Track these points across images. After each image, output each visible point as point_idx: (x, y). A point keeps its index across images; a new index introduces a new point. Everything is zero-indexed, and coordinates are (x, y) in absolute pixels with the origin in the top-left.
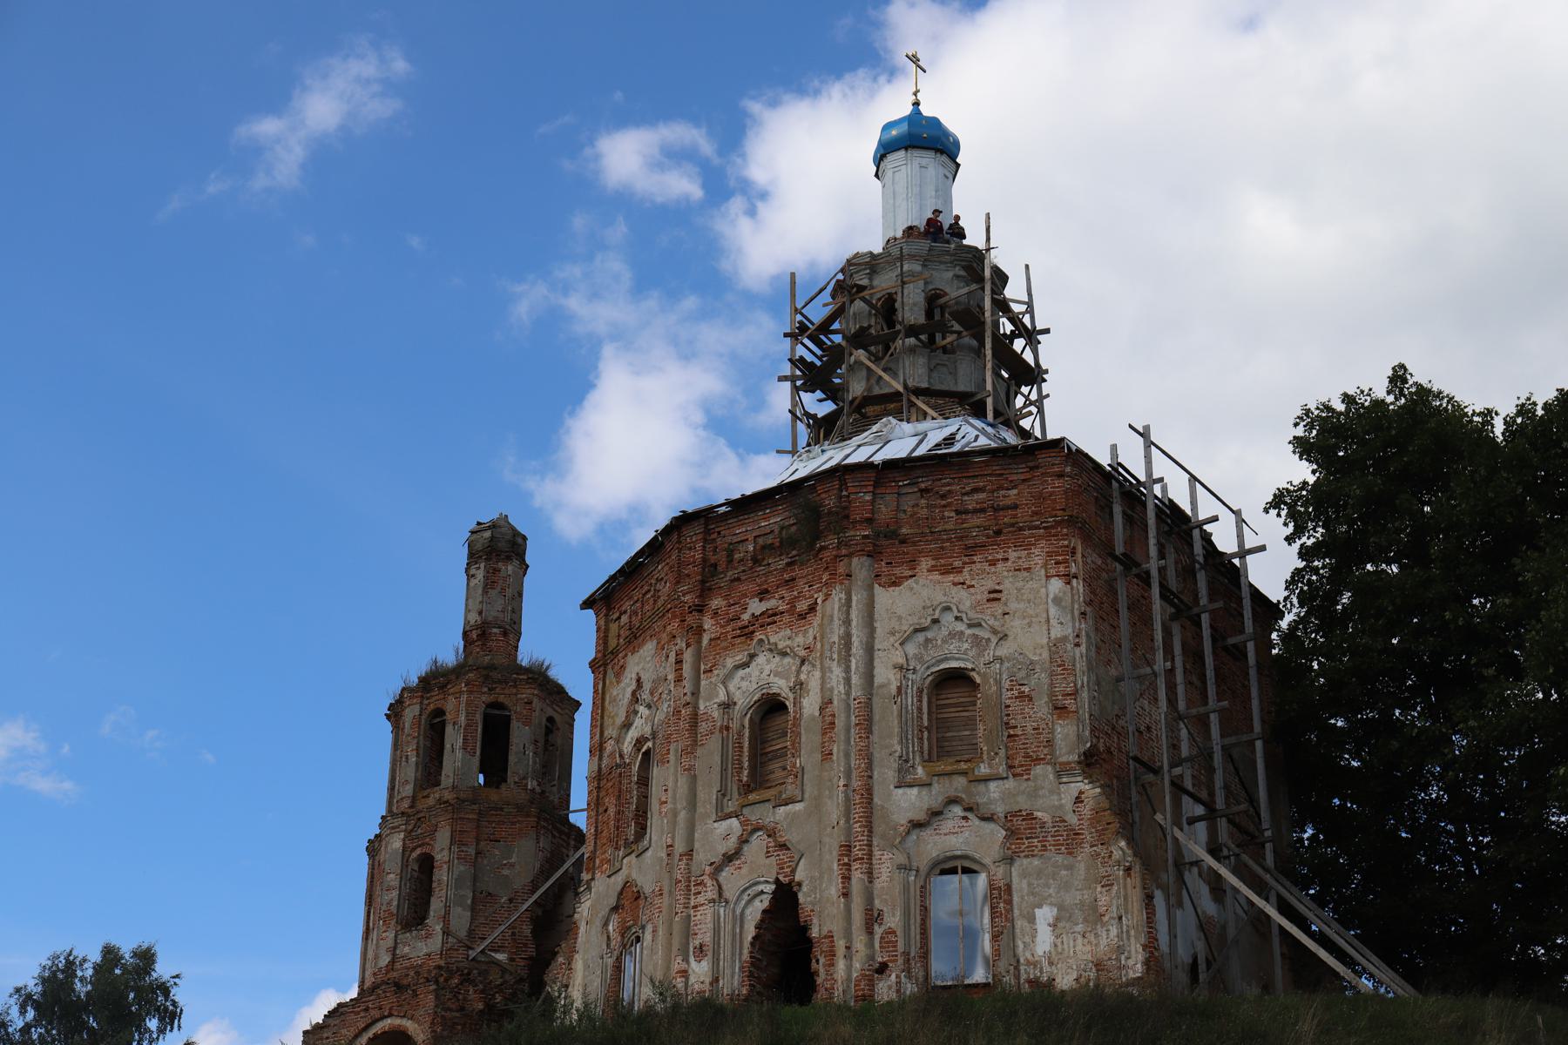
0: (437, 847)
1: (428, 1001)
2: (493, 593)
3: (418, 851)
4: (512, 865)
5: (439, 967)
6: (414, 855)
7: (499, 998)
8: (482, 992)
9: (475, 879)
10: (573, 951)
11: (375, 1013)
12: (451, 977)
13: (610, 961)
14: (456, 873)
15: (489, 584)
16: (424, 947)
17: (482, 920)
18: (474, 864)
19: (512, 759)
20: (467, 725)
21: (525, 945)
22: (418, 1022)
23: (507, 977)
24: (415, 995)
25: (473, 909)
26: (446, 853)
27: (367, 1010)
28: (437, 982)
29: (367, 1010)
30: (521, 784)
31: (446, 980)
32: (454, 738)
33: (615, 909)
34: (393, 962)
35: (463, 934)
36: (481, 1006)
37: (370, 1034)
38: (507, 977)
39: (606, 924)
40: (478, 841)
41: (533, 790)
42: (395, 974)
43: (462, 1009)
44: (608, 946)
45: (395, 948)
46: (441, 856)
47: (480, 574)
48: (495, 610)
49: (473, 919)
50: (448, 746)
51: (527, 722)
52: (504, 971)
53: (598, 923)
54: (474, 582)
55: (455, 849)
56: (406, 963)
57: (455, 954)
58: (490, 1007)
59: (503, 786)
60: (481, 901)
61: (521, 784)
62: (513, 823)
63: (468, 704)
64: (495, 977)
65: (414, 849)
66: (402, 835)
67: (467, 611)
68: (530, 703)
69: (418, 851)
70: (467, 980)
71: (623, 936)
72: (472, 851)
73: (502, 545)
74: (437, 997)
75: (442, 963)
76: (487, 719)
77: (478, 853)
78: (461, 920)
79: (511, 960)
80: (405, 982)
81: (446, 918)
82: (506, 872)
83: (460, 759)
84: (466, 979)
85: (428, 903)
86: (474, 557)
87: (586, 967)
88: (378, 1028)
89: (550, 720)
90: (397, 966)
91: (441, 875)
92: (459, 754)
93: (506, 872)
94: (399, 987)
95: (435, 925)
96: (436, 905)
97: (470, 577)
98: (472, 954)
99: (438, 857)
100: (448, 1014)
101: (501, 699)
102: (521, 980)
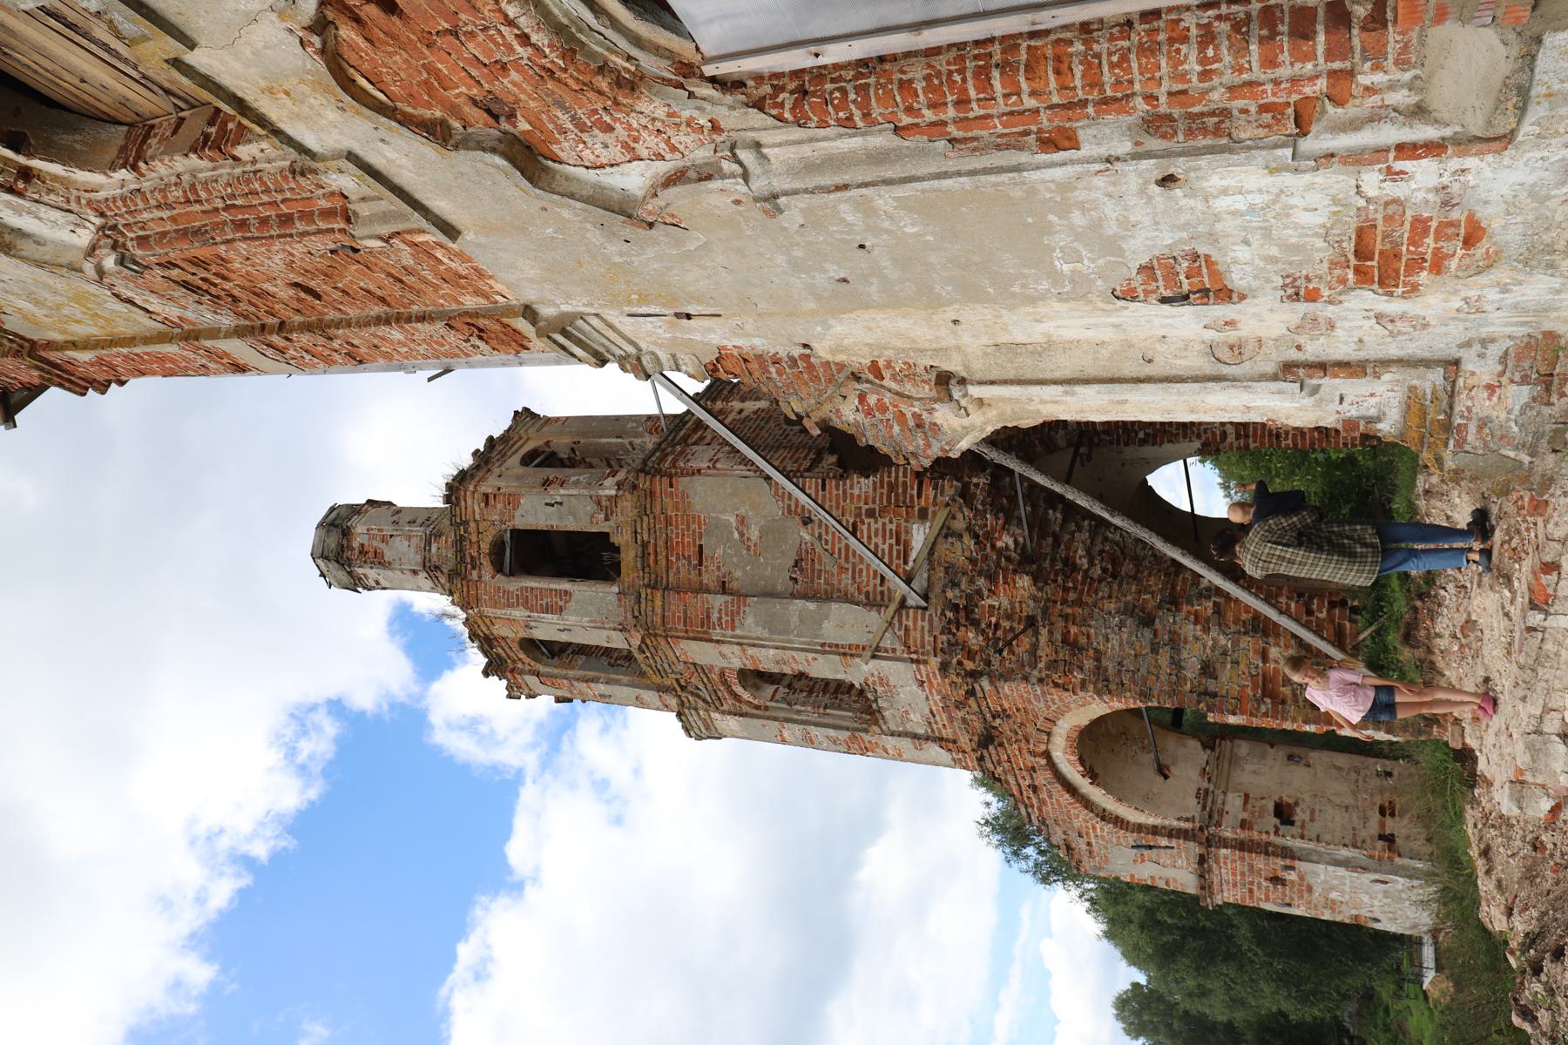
0: (720, 664)
1: (1013, 693)
2: (388, 555)
3: (738, 689)
4: (742, 520)
5: (944, 668)
6: (746, 696)
7: (1006, 541)
8: (991, 578)
9: (770, 594)
10: (804, 363)
11: (1043, 777)
12: (972, 652)
13: (784, 147)
14: (759, 632)
15: (379, 561)
16: (908, 691)
17: (846, 579)
18: (741, 595)
19: (570, 525)
20: (526, 605)
21: (892, 487)
22: (1061, 713)
23: (959, 524)
24: (1004, 714)
25: (826, 596)
26: (725, 649)
27: (1035, 789)
28: (974, 675)
29: (1035, 789)
30: (608, 508)
31: (971, 655)
32: (547, 629)
33: (529, 159)
34: (940, 740)
35: (874, 620)
36: (1024, 582)
37: (1084, 785)
38: (959, 524)
39: (621, 208)
40: (702, 589)
41: (619, 485)
42: (964, 741)
43: (1031, 622)
44: (706, 175)
45: (915, 736)
46: (735, 659)
47: (372, 573)
48: (404, 549)
49: (847, 598)
50: (564, 637)
51: (512, 501)
52: (947, 532)
53: (651, 255)
54: (384, 583)
55: (716, 634)
56: (942, 718)
57: (915, 635)
58: (1027, 561)
59: (616, 539)
60: (809, 582)
61: (608, 508)
62: (668, 521)
63: (495, 605)
64: (960, 551)
65: (736, 697)
66: (715, 715)
67: (419, 589)
68: (486, 496)
69: (738, 689)
70: (968, 610)
71: (631, 84)
72: (718, 601)
73: (333, 541)
74: (1007, 676)
75: (935, 662)
76: (511, 574)
77: (724, 588)
78: (847, 622)
79: (923, 515)
80: (978, 725)
81: (847, 652)
82: (754, 534)
83: (584, 613)
84: (965, 613)
85: (826, 683)
86: (355, 584)
87: (845, 293)
88: (1073, 772)
89: (527, 460)
90: (947, 733)
91: (767, 659)
92: (571, 619)
93: (754, 534)
94: (987, 739)
95: (859, 672)
96: (824, 668)
97: (378, 585)
98: (914, 600)
99: (737, 664)
100: (1044, 651)
101: (485, 547)
102: (965, 494)
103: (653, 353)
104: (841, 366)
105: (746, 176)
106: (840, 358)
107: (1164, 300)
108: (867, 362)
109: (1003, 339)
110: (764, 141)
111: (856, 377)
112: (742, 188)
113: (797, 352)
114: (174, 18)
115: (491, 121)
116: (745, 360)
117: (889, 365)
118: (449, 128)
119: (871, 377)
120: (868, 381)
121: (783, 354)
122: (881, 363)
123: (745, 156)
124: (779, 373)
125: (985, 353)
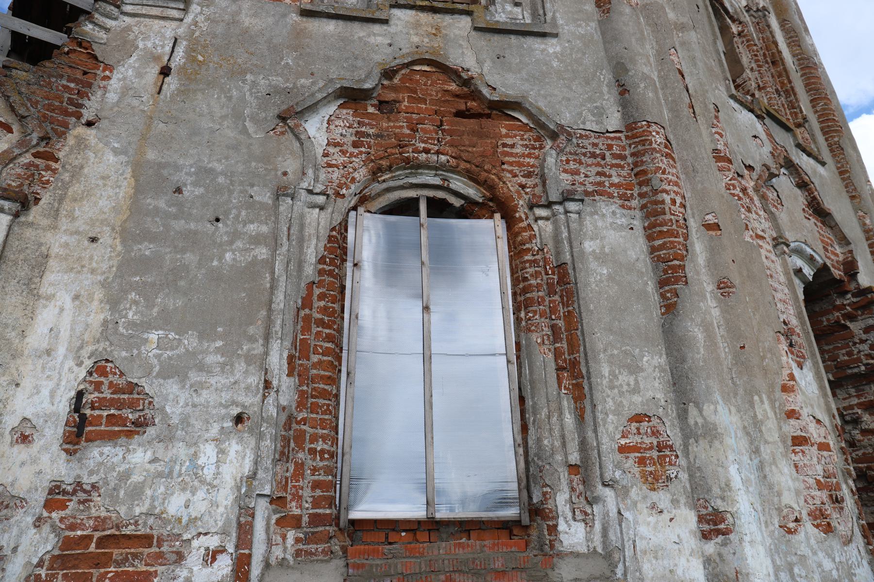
71: (375, 174)
103: (116, 19)
104: (62, 135)
105: (310, 192)
106: (71, 141)
107: (80, 395)
108: (61, 155)
109: (52, 263)
110: (323, 213)
111: (45, 138)
112: (305, 185)
113: (88, 114)
114: (488, 36)
115: (382, 99)
116: (85, 73)
117: (48, 168)
118: (386, 79)
119: (41, 149)
120: (38, 144)
121: (86, 102)
122: (54, 165)
123: (321, 199)
124: (66, 87)
125: (40, 245)
